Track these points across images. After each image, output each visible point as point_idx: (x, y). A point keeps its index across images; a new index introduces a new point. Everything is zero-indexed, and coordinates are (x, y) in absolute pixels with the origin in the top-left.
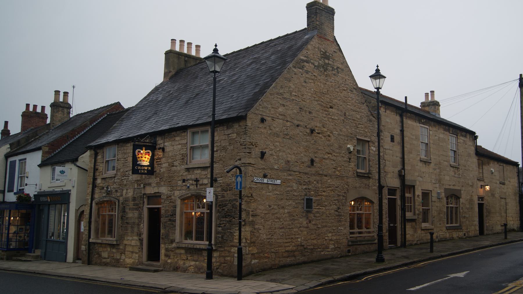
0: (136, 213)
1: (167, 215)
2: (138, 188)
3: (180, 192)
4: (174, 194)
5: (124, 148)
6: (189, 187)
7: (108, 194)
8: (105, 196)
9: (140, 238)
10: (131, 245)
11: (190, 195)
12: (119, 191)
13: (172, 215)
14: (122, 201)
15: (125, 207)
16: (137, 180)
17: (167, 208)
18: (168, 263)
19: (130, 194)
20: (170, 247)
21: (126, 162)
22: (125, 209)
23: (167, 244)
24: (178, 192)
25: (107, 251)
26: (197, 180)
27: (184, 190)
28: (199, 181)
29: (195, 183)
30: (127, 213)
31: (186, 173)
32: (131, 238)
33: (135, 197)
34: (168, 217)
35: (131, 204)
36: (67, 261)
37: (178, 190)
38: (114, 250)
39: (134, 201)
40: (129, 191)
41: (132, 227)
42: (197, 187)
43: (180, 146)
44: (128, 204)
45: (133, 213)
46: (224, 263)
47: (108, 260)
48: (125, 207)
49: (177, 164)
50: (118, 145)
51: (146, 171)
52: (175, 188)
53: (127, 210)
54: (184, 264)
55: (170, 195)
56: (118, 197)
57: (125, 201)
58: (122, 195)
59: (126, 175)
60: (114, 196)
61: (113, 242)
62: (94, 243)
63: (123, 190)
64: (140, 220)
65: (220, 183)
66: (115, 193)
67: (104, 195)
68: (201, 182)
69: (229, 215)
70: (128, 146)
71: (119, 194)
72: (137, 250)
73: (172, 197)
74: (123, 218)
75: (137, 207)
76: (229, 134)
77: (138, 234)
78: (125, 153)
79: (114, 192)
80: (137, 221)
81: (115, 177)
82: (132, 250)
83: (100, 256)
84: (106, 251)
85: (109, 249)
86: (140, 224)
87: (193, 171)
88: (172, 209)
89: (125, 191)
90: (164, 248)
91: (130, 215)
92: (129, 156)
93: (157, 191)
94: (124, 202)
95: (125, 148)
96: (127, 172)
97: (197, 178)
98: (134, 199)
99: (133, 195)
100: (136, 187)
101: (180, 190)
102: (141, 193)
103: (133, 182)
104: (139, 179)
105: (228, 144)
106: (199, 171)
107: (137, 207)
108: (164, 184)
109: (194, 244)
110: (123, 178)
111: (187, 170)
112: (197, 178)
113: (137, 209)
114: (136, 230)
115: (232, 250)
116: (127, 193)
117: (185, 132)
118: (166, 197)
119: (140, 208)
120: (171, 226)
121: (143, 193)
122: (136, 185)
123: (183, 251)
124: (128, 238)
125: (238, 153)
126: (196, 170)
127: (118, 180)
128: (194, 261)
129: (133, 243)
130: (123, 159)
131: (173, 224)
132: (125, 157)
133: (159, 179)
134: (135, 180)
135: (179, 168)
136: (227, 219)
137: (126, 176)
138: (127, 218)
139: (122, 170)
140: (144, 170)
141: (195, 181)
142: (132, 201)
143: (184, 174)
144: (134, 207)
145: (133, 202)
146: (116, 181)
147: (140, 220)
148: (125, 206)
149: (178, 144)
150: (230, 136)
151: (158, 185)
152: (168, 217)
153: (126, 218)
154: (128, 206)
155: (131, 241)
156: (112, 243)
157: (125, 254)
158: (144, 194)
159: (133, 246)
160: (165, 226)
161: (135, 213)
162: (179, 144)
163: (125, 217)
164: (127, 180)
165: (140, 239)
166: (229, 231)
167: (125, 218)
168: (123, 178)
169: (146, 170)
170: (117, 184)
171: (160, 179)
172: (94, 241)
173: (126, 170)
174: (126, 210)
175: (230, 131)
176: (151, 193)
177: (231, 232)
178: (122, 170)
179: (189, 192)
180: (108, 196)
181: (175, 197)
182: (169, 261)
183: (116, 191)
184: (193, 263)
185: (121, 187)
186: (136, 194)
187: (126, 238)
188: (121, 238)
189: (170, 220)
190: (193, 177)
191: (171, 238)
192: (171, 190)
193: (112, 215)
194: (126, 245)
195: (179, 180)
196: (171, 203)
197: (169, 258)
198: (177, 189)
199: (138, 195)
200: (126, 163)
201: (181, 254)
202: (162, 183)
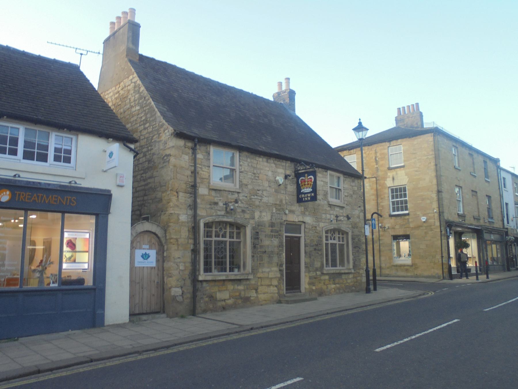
0: (276, 242)
1: (312, 245)
2: (277, 213)
3: (324, 224)
4: (319, 225)
5: (252, 160)
6: (332, 221)
7: (227, 212)
8: (223, 216)
9: (281, 268)
10: (268, 278)
11: (332, 228)
12: (248, 212)
13: (317, 245)
14: (254, 225)
15: (257, 233)
16: (275, 204)
17: (312, 238)
18: (313, 290)
19: (266, 217)
20: (313, 275)
21: (257, 178)
22: (258, 235)
23: (312, 273)
24: (322, 223)
25: (227, 290)
26: (337, 216)
27: (327, 223)
28: (338, 217)
29: (336, 218)
30: (261, 240)
31: (328, 209)
32: (267, 270)
33: (274, 223)
34: (313, 246)
35: (268, 230)
36: (107, 323)
37: (323, 222)
38: (241, 287)
39: (272, 227)
40: (264, 214)
41: (269, 257)
42: (337, 221)
43: (322, 183)
44: (263, 230)
45: (271, 241)
46: (356, 282)
47: (230, 302)
48: (257, 233)
49: (321, 198)
50: (240, 152)
51: (309, 198)
52: (320, 220)
53: (262, 236)
54: (327, 288)
55: (315, 226)
56: (246, 219)
57: (258, 226)
58: (253, 218)
59: (258, 195)
60: (239, 216)
61: (248, 277)
62: (201, 281)
63: (254, 212)
64: (281, 249)
65: (351, 222)
66: (241, 214)
67: (223, 213)
68: (339, 219)
69: (357, 246)
70: (260, 161)
71: (247, 216)
72: (275, 282)
73: (318, 228)
74: (256, 246)
75: (276, 234)
76: (353, 186)
77: (278, 265)
78: (255, 167)
79: (239, 212)
80: (276, 250)
81: (238, 193)
82: (270, 284)
83: (212, 298)
84: (224, 290)
85: (230, 287)
86: (282, 254)
87: (335, 208)
88: (317, 239)
89: (257, 214)
90: (308, 277)
91: (266, 242)
92: (260, 173)
93: (302, 220)
94: (257, 226)
95: (255, 162)
96: (258, 190)
97: (337, 215)
98: (272, 225)
99: (271, 220)
100: (274, 211)
101: (324, 222)
102: (282, 219)
103: (269, 204)
104: (278, 203)
105: (352, 193)
106: (337, 209)
107: (276, 234)
108: (309, 214)
109: (340, 270)
110: (253, 197)
111: (329, 206)
112: (337, 215)
113: (275, 236)
114: (275, 259)
115: (361, 272)
116: (260, 216)
117: (326, 172)
118: (311, 227)
119: (280, 235)
120: (317, 255)
121: (284, 219)
122: (274, 209)
123: (327, 277)
124: (264, 270)
125: (359, 202)
126: (336, 207)
127: (244, 198)
128: (335, 284)
129: (271, 275)
130: (251, 174)
131: (318, 253)
132: (255, 172)
133: (303, 208)
134: (273, 204)
135: (322, 202)
136: (356, 249)
137: (256, 196)
138: (261, 247)
139: (250, 187)
140: (307, 197)
141: (335, 217)
142: (269, 227)
143: (327, 209)
144: (272, 234)
145: (270, 228)
146: (241, 198)
147: (281, 249)
148: (258, 231)
149: (321, 180)
150: (353, 187)
151: (303, 214)
152: (313, 246)
153: (260, 246)
154: (262, 231)
155: (268, 273)
156: (246, 278)
157: (256, 290)
158: (284, 221)
159: (271, 279)
160: (310, 254)
161: (274, 241)
162: (322, 181)
163: (258, 245)
164: (260, 200)
165: (280, 270)
166: (358, 258)
167: (258, 246)
168: (253, 197)
169: (309, 197)
170: (244, 203)
171: (304, 208)
172: (209, 277)
173: (257, 188)
174: (260, 237)
175: (353, 184)
176: (293, 221)
177: (359, 259)
178: (250, 187)
179: (332, 225)
180: (227, 215)
181: (320, 228)
182: (314, 288)
183: (243, 211)
184: (333, 286)
185: (250, 208)
186: (275, 219)
187: (260, 270)
188: (254, 271)
189: (315, 249)
190: (335, 213)
191: (316, 266)
192: (316, 221)
193: (222, 242)
194: (259, 278)
195: (323, 214)
196: (316, 234)
197: (314, 285)
198: (321, 221)
199: (279, 221)
200: (256, 179)
201: (325, 280)
202: (307, 213)
